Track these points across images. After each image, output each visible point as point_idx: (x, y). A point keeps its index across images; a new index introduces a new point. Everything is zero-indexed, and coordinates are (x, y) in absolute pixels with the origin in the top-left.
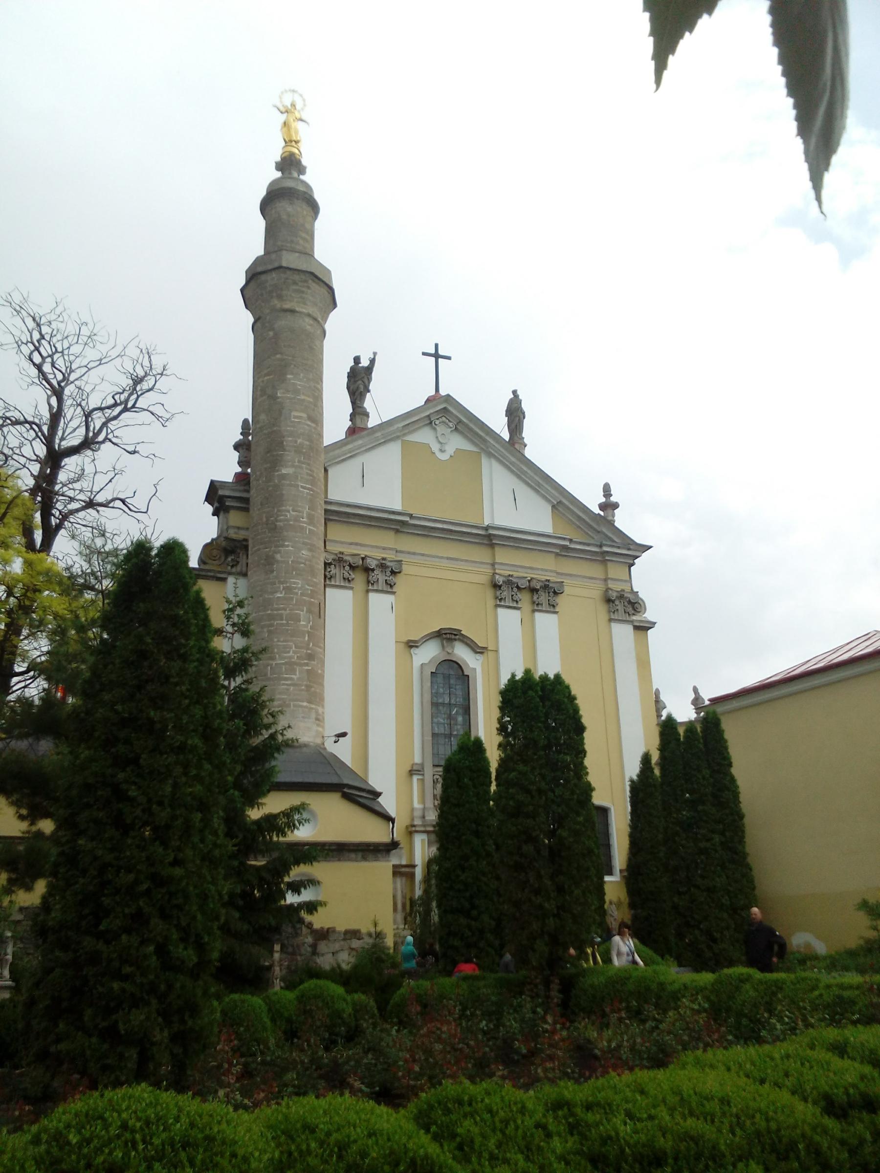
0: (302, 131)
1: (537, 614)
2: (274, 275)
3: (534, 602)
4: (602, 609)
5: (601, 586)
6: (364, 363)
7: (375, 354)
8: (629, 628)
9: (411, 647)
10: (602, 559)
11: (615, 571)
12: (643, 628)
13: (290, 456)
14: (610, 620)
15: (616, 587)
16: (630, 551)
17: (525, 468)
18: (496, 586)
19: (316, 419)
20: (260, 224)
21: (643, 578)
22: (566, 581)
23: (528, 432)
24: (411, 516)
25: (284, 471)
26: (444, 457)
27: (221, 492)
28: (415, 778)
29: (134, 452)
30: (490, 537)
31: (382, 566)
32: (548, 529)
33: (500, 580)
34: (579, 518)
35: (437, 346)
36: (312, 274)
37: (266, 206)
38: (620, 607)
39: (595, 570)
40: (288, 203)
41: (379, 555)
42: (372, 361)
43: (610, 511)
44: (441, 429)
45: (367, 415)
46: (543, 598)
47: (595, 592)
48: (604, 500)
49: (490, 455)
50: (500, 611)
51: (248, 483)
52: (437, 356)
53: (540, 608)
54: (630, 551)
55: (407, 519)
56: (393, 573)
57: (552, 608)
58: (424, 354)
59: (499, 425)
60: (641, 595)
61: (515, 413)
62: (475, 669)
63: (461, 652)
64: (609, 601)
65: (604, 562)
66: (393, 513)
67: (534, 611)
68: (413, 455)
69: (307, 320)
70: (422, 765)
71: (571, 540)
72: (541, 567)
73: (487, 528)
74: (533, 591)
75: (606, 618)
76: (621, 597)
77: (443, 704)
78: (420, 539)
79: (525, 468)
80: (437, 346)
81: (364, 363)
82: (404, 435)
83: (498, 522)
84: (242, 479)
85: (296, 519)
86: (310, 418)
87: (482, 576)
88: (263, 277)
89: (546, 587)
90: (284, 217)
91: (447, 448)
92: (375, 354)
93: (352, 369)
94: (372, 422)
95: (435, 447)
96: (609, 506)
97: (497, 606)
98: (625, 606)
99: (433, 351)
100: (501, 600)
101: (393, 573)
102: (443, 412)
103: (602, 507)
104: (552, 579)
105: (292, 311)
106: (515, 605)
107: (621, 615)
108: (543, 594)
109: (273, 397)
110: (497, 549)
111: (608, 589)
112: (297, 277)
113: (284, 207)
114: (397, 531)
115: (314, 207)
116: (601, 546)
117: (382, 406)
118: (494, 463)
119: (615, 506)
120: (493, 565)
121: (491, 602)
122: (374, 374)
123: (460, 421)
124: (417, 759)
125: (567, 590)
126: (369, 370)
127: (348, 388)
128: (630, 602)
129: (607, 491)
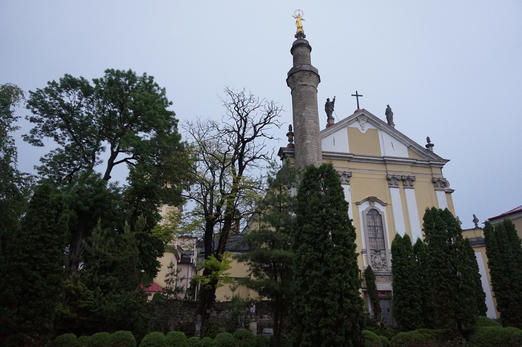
1: (406, 189)
3: (404, 185)
4: (432, 186)
5: (430, 177)
6: (331, 100)
7: (335, 97)
8: (443, 193)
9: (358, 205)
10: (430, 166)
11: (435, 171)
12: (449, 192)
13: (309, 136)
14: (435, 190)
15: (437, 177)
16: (441, 162)
18: (388, 179)
19: (317, 122)
20: (291, 57)
21: (447, 172)
22: (416, 176)
23: (395, 120)
24: (354, 155)
25: (307, 142)
26: (364, 132)
27: (284, 152)
28: (364, 255)
29: (272, 138)
30: (384, 161)
31: (344, 174)
32: (407, 157)
33: (390, 177)
34: (419, 151)
35: (357, 92)
36: (312, 71)
37: (292, 51)
38: (439, 185)
39: (427, 171)
40: (300, 47)
41: (343, 170)
42: (334, 100)
43: (430, 148)
44: (361, 122)
45: (334, 119)
46: (408, 183)
47: (428, 179)
48: (427, 143)
49: (381, 130)
50: (391, 189)
51: (294, 147)
52: (357, 95)
54: (441, 162)
55: (352, 156)
56: (348, 177)
57: (412, 187)
58: (352, 95)
59: (383, 118)
60: (447, 180)
61: (389, 113)
62: (383, 212)
63: (377, 206)
64: (434, 182)
65: (431, 167)
66: (347, 154)
67: (404, 188)
68: (352, 133)
69: (311, 88)
70: (366, 250)
71: (417, 160)
72: (406, 171)
73: (383, 157)
74: (403, 180)
75: (434, 189)
76: (439, 180)
77: (372, 226)
78: (357, 163)
80: (357, 92)
81: (331, 100)
83: (387, 155)
84: (291, 146)
85: (313, 159)
86: (315, 122)
87: (383, 176)
88: (295, 74)
89: (408, 178)
90: (300, 53)
91: (364, 128)
92: (335, 97)
93: (326, 103)
94: (336, 122)
95: (360, 128)
96: (430, 146)
97: (389, 187)
98: (441, 184)
99: (355, 94)
101: (348, 177)
102: (361, 115)
103: (427, 146)
104: (411, 175)
105: (306, 85)
107: (440, 188)
108: (407, 182)
109: (302, 116)
110: (388, 165)
111: (433, 178)
113: (300, 50)
114: (349, 161)
115: (310, 48)
116: (429, 161)
117: (338, 115)
118: (383, 133)
119: (433, 145)
120: (386, 171)
121: (387, 186)
122: (335, 104)
123: (369, 118)
124: (364, 248)
125: (417, 179)
126: (333, 103)
127: (326, 110)
128: (443, 182)
129: (428, 140)
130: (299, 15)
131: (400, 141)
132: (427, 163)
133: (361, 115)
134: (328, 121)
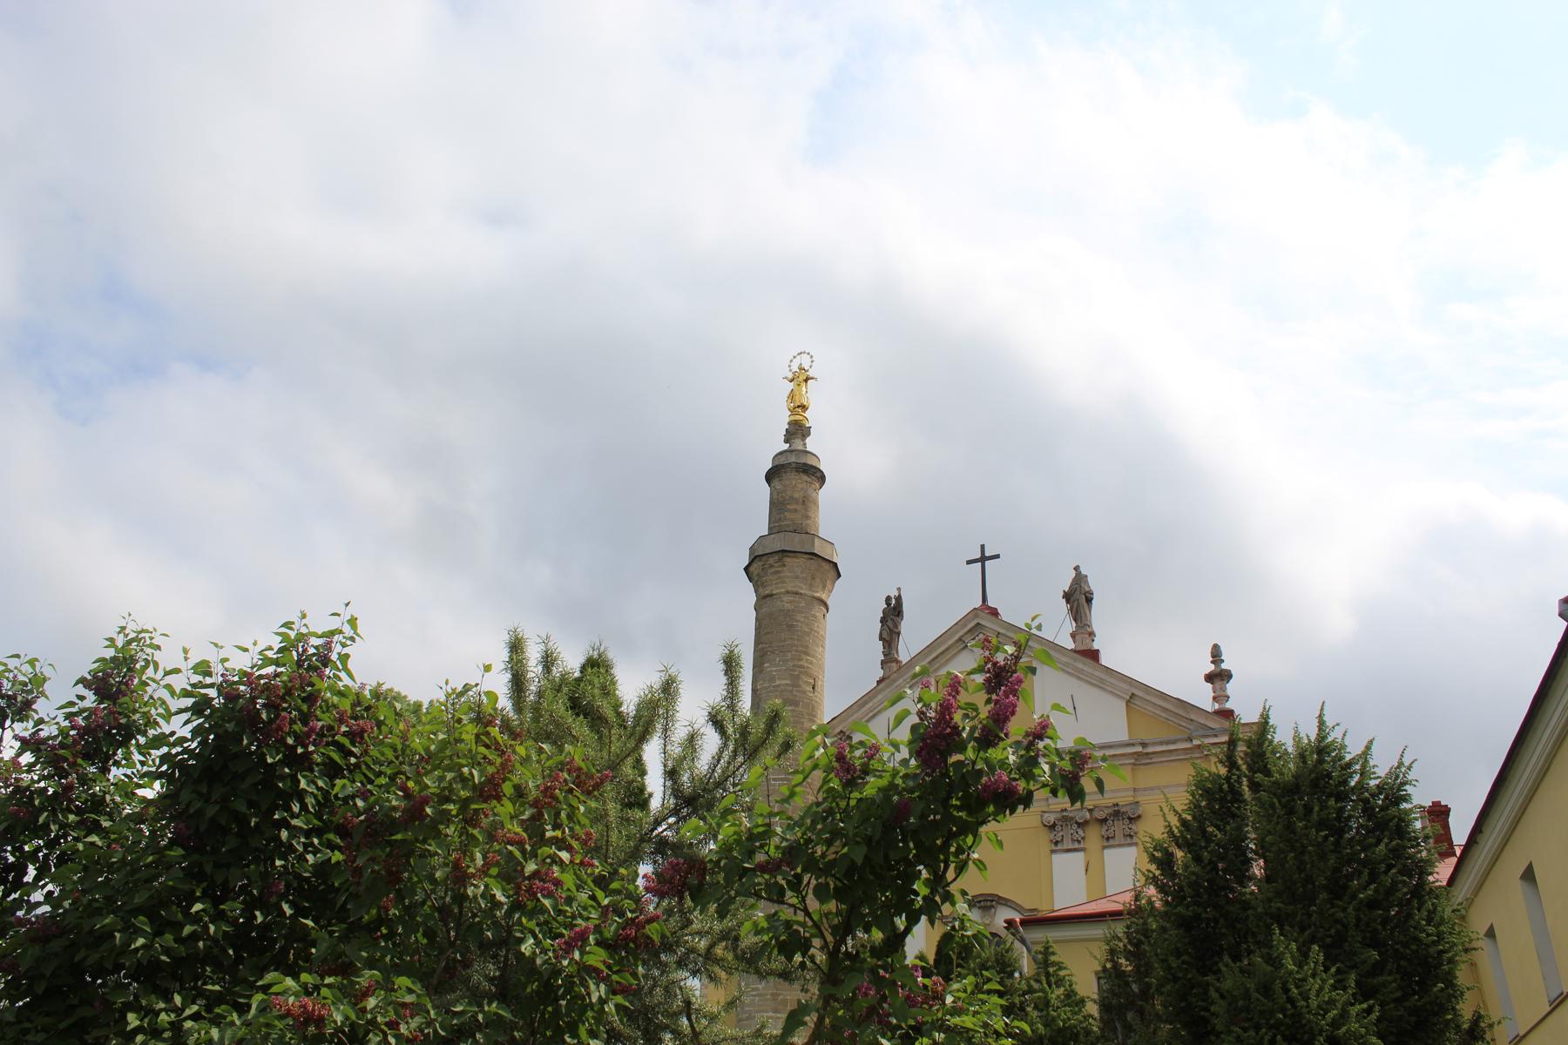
0: (813, 395)
2: (755, 565)
17: (1080, 666)
33: (1051, 818)
35: (983, 547)
42: (899, 599)
46: (1119, 827)
48: (1212, 667)
53: (1111, 842)
61: (1078, 598)
71: (1144, 745)
79: (1080, 666)
80: (983, 547)
82: (936, 670)
89: (1117, 814)
96: (1218, 677)
97: (1053, 852)
100: (1056, 843)
102: (982, 623)
103: (1210, 678)
106: (1076, 845)
112: (771, 561)
117: (911, 643)
130: (801, 369)
131: (1100, 685)
132: (1187, 745)
133: (982, 623)
134: (883, 662)
